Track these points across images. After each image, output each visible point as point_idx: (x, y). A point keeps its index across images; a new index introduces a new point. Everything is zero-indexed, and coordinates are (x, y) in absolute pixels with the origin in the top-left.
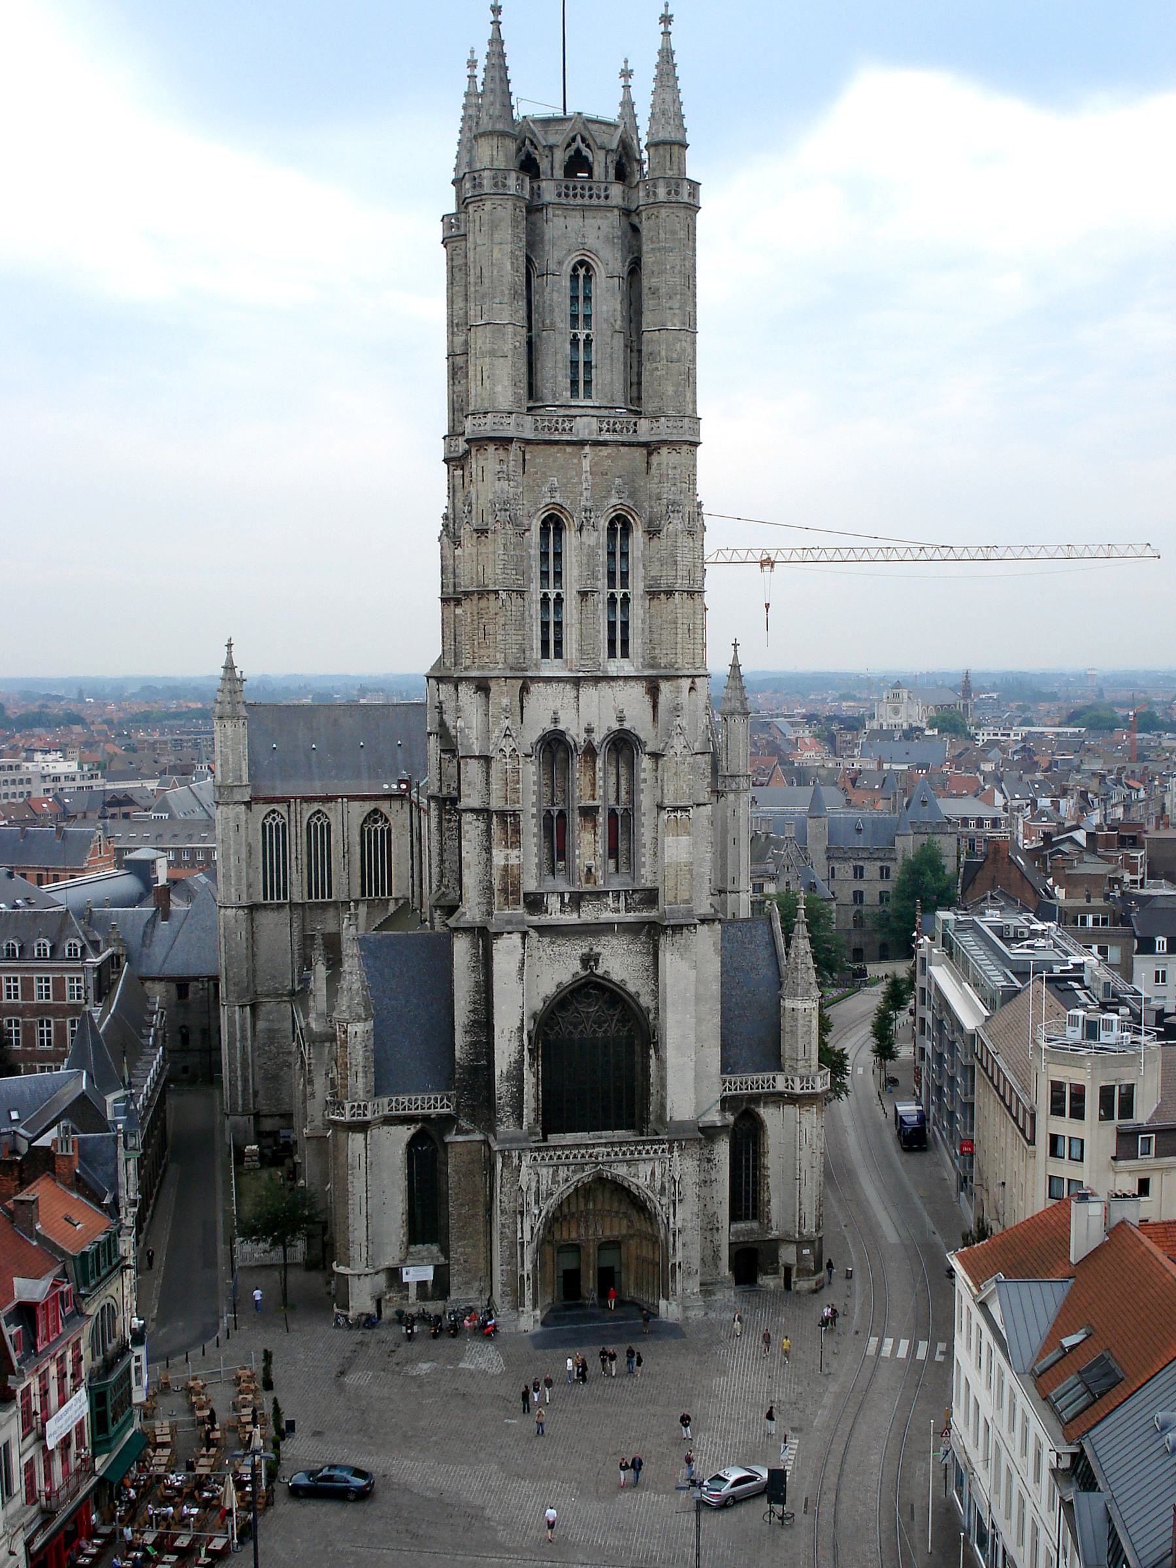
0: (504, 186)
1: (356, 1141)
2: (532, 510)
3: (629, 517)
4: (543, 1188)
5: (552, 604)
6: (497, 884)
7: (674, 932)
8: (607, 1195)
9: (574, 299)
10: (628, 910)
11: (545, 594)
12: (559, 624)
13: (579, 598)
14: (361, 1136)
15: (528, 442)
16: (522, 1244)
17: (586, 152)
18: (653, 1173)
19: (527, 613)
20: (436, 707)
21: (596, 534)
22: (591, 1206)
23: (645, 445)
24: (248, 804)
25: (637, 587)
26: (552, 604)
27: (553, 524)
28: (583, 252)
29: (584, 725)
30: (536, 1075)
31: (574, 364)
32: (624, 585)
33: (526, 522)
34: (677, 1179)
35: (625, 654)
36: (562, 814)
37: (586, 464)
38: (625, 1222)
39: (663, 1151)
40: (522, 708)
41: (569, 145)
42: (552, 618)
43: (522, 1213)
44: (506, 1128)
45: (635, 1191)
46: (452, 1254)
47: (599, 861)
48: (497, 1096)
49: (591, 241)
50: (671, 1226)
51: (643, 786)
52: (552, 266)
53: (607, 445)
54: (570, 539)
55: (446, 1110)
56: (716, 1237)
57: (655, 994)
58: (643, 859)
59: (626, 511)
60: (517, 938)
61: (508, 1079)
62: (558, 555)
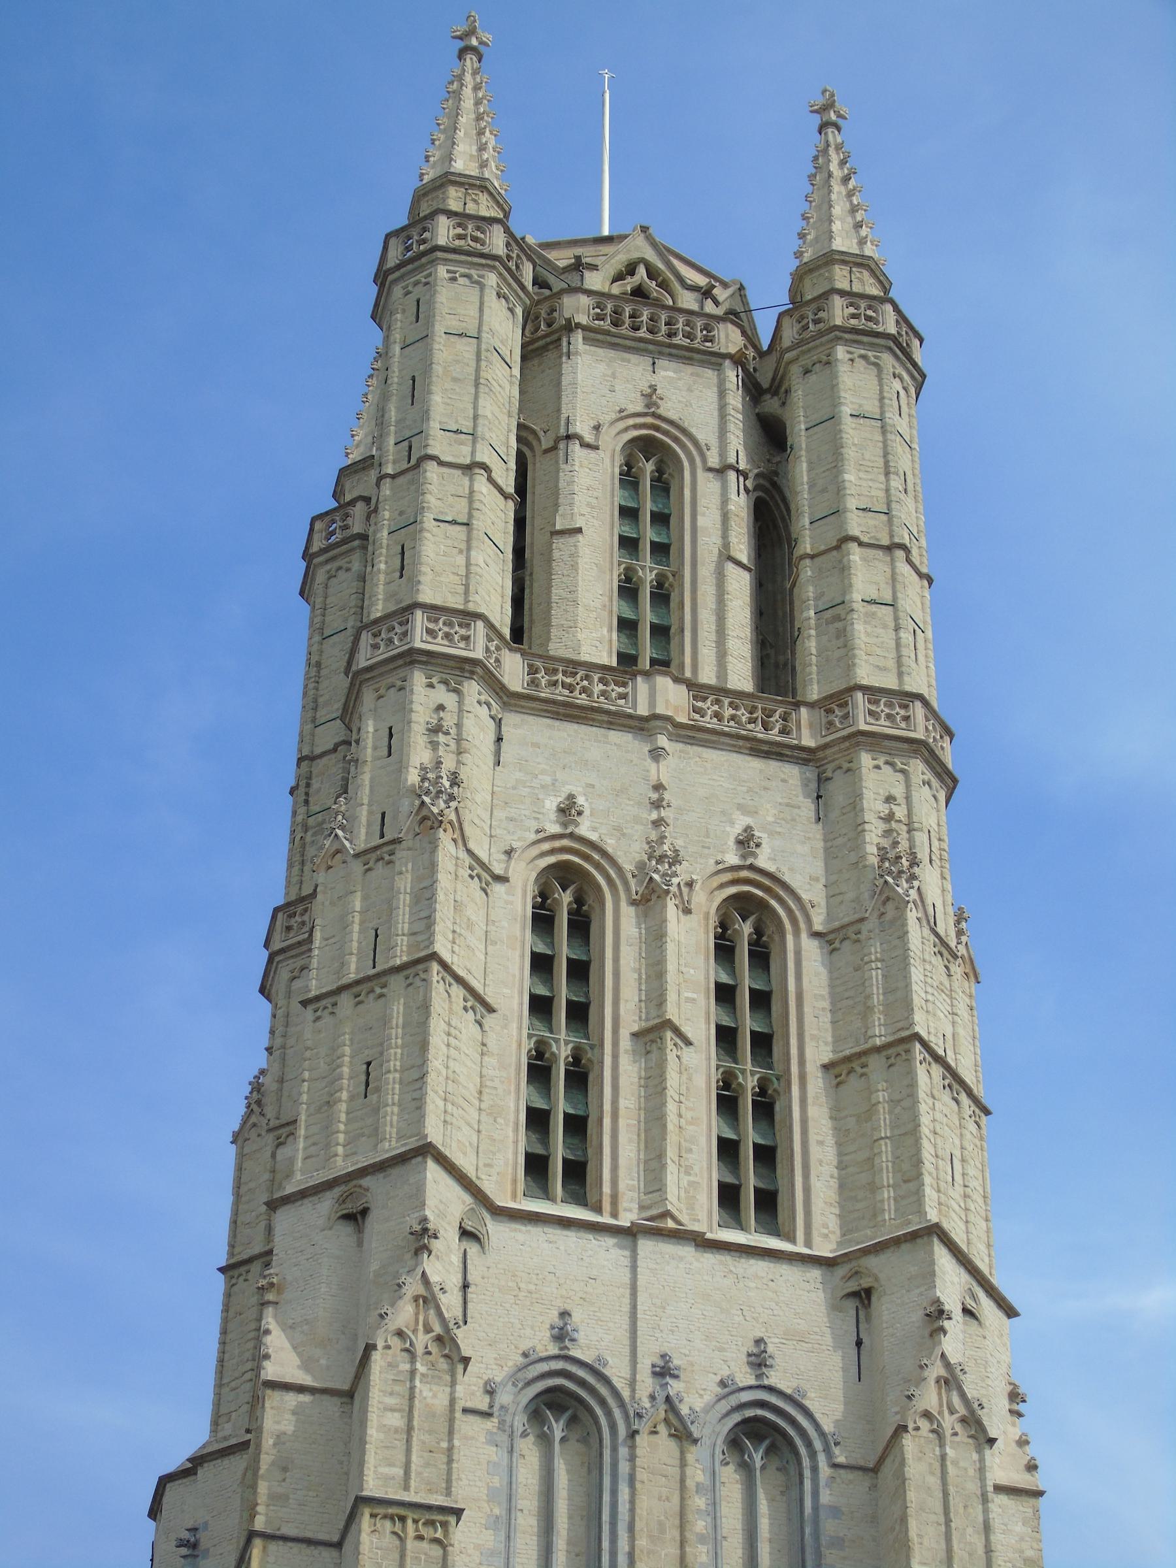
3: (773, 903)
20: (182, 1543)
28: (649, 420)
41: (618, 278)
49: (670, 408)
52: (582, 428)
59: (767, 890)
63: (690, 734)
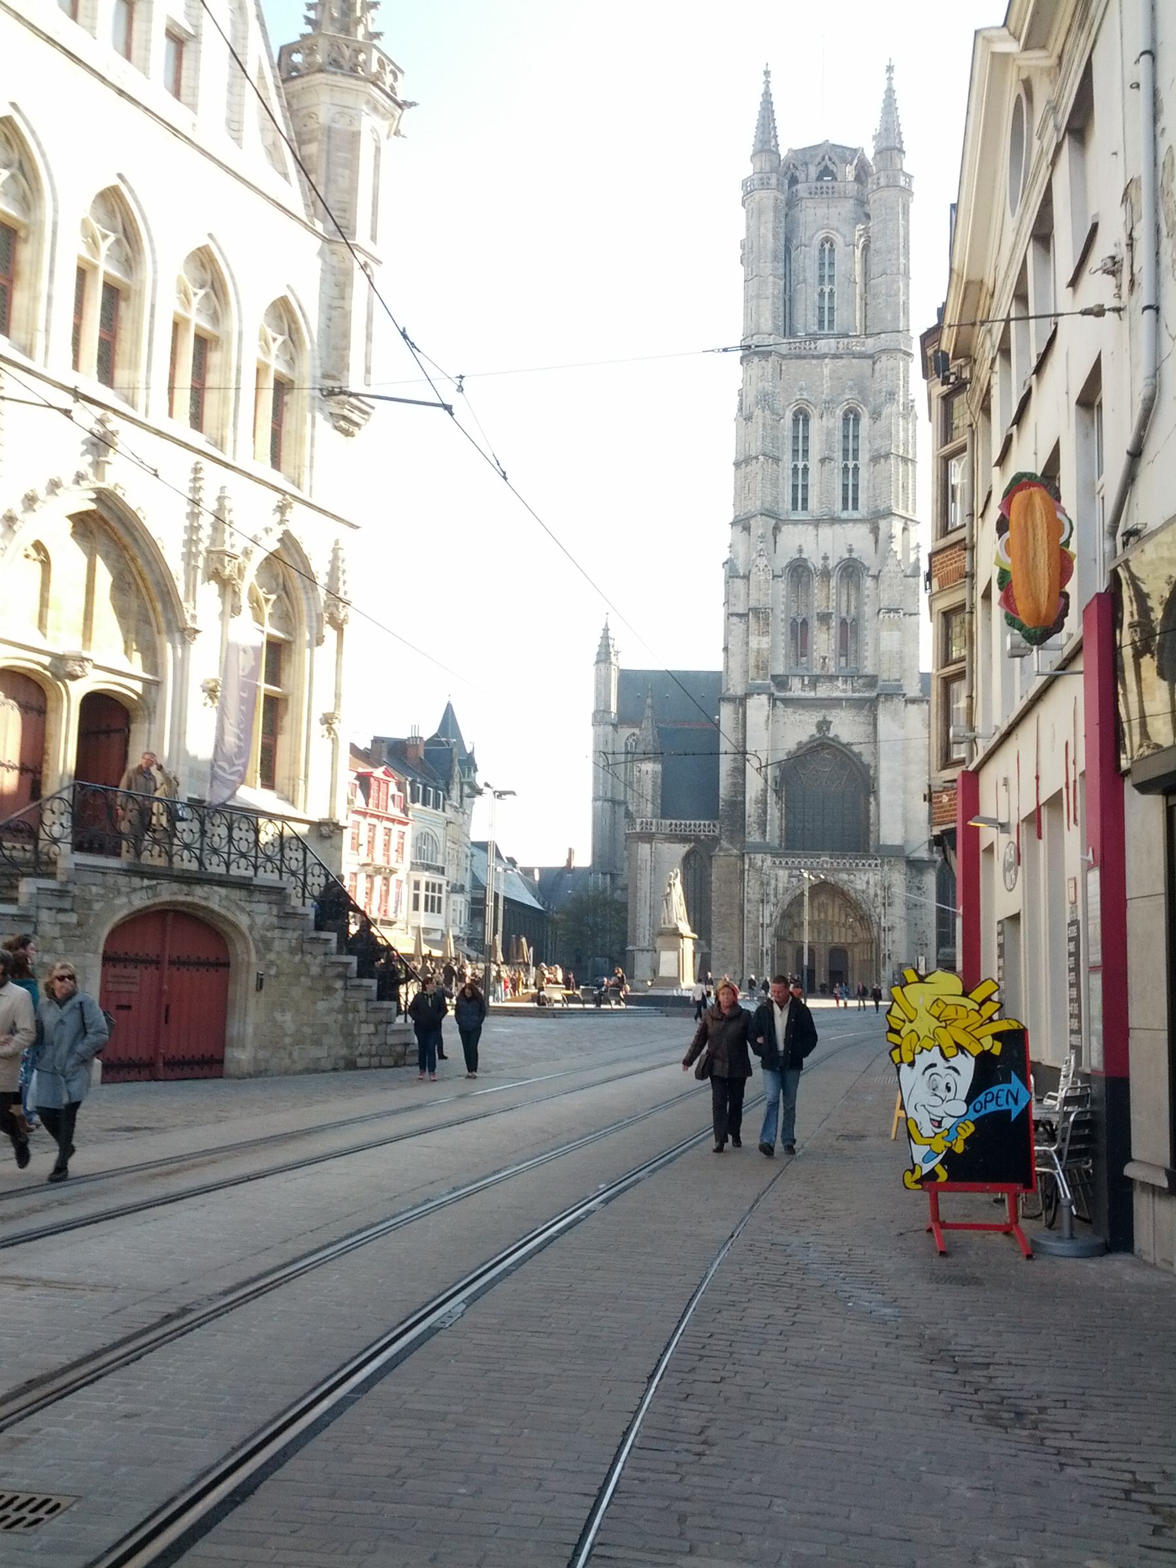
0: (768, 183)
1: (644, 849)
2: (787, 404)
4: (780, 885)
5: (800, 472)
6: (752, 662)
7: (886, 700)
8: (837, 910)
9: (822, 265)
10: (854, 691)
11: (796, 466)
12: (805, 487)
13: (820, 465)
14: (648, 846)
15: (784, 357)
16: (762, 925)
17: (831, 167)
18: (868, 883)
19: (780, 478)
21: (833, 420)
22: (822, 915)
23: (871, 356)
24: (615, 726)
25: (864, 457)
26: (800, 472)
27: (801, 417)
29: (822, 555)
30: (780, 810)
31: (821, 309)
32: (856, 458)
33: (781, 412)
34: (886, 884)
35: (855, 508)
36: (805, 623)
37: (826, 371)
38: (850, 932)
39: (876, 865)
40: (775, 543)
42: (800, 482)
43: (762, 901)
44: (754, 837)
45: (853, 895)
46: (713, 943)
47: (831, 655)
48: (747, 815)
49: (834, 223)
50: (883, 925)
51: (866, 600)
53: (842, 358)
54: (814, 424)
55: (712, 833)
56: (925, 949)
57: (876, 754)
58: (866, 654)
60: (764, 698)
61: (756, 802)
62: (806, 438)
63: (836, 356)
